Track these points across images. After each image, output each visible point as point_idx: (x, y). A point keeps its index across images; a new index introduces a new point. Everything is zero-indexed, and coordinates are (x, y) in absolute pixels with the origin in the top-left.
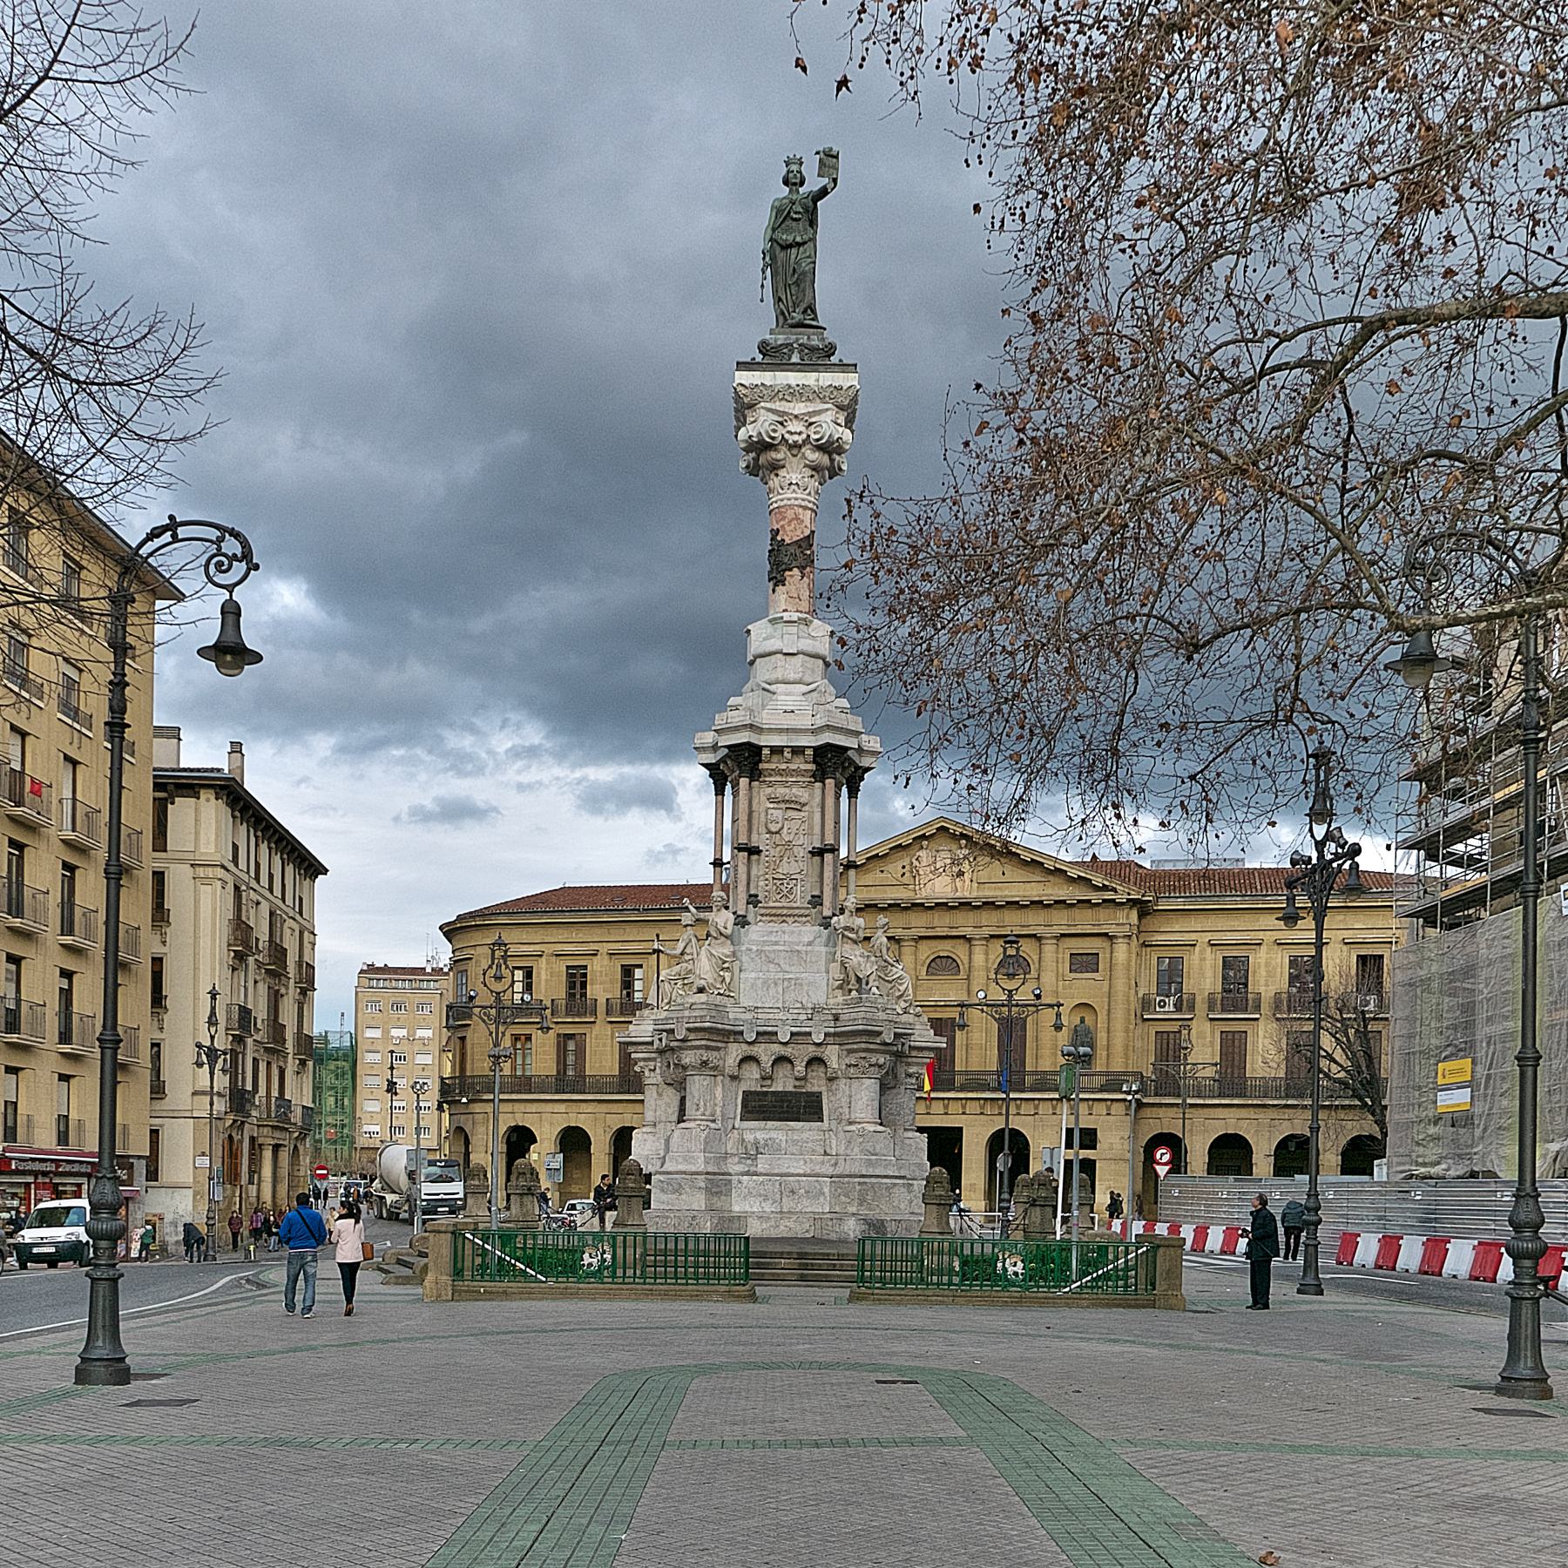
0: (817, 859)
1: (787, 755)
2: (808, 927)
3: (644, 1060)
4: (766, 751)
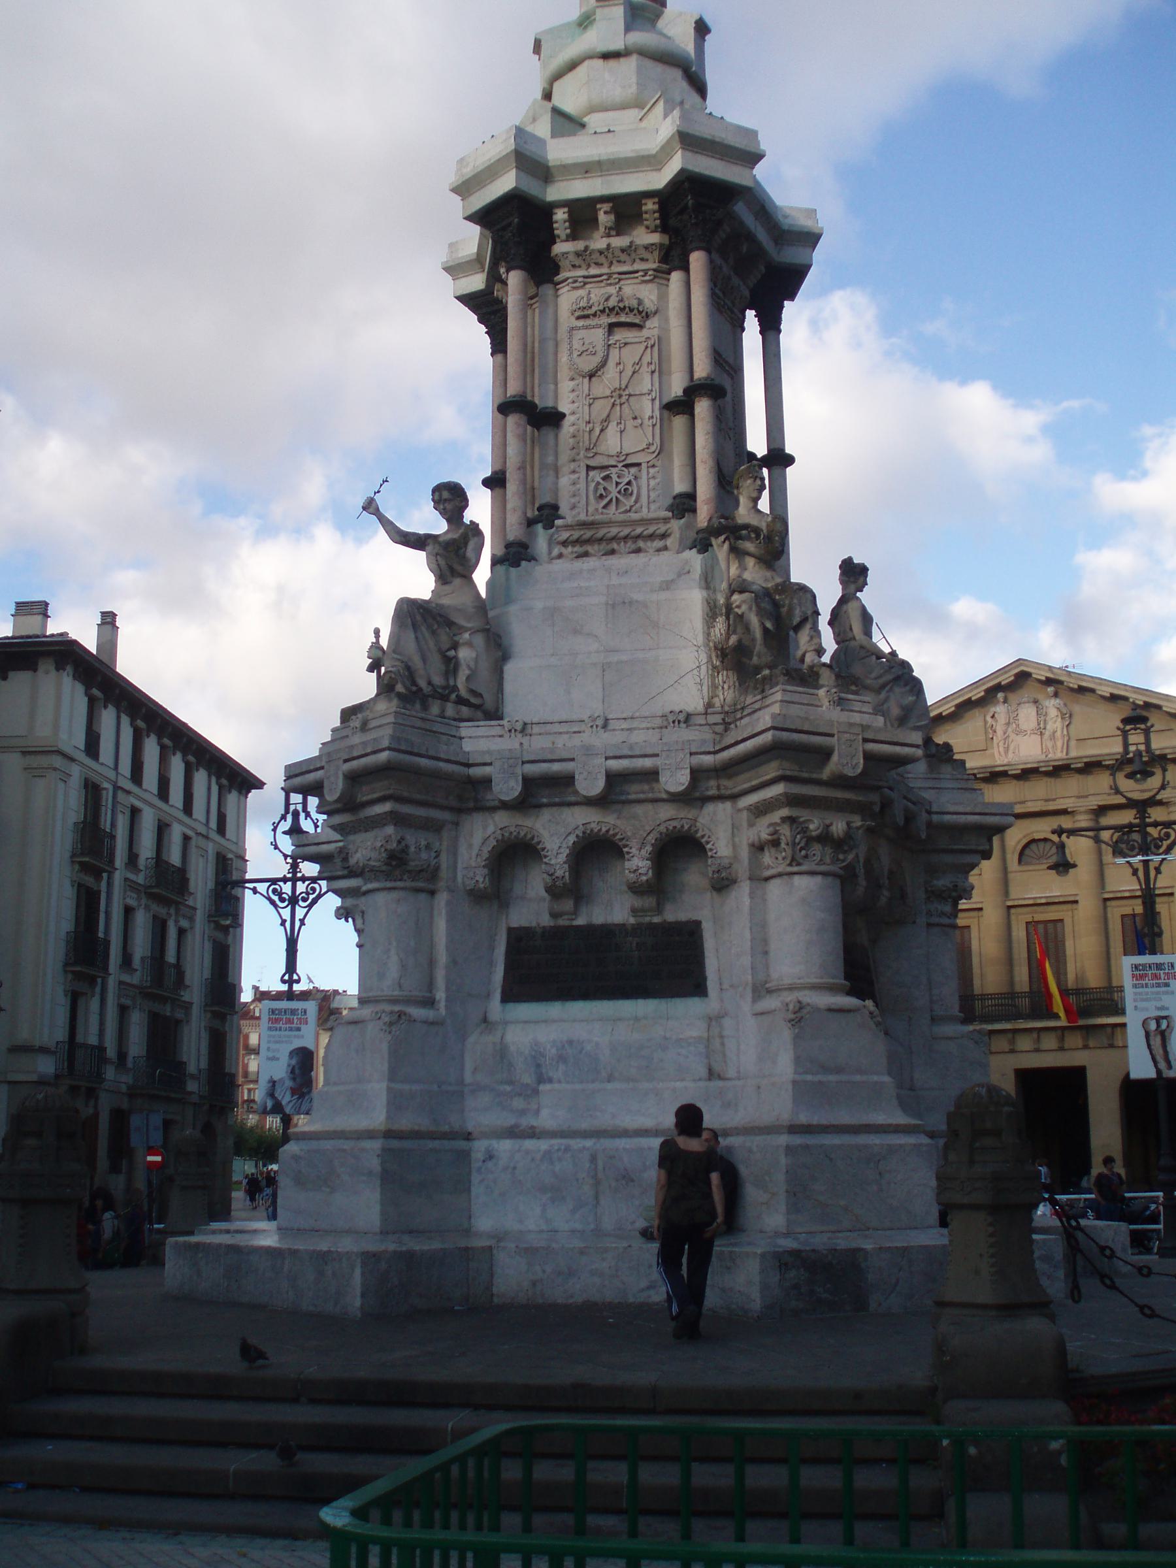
0: (679, 422)
1: (604, 218)
4: (560, 215)
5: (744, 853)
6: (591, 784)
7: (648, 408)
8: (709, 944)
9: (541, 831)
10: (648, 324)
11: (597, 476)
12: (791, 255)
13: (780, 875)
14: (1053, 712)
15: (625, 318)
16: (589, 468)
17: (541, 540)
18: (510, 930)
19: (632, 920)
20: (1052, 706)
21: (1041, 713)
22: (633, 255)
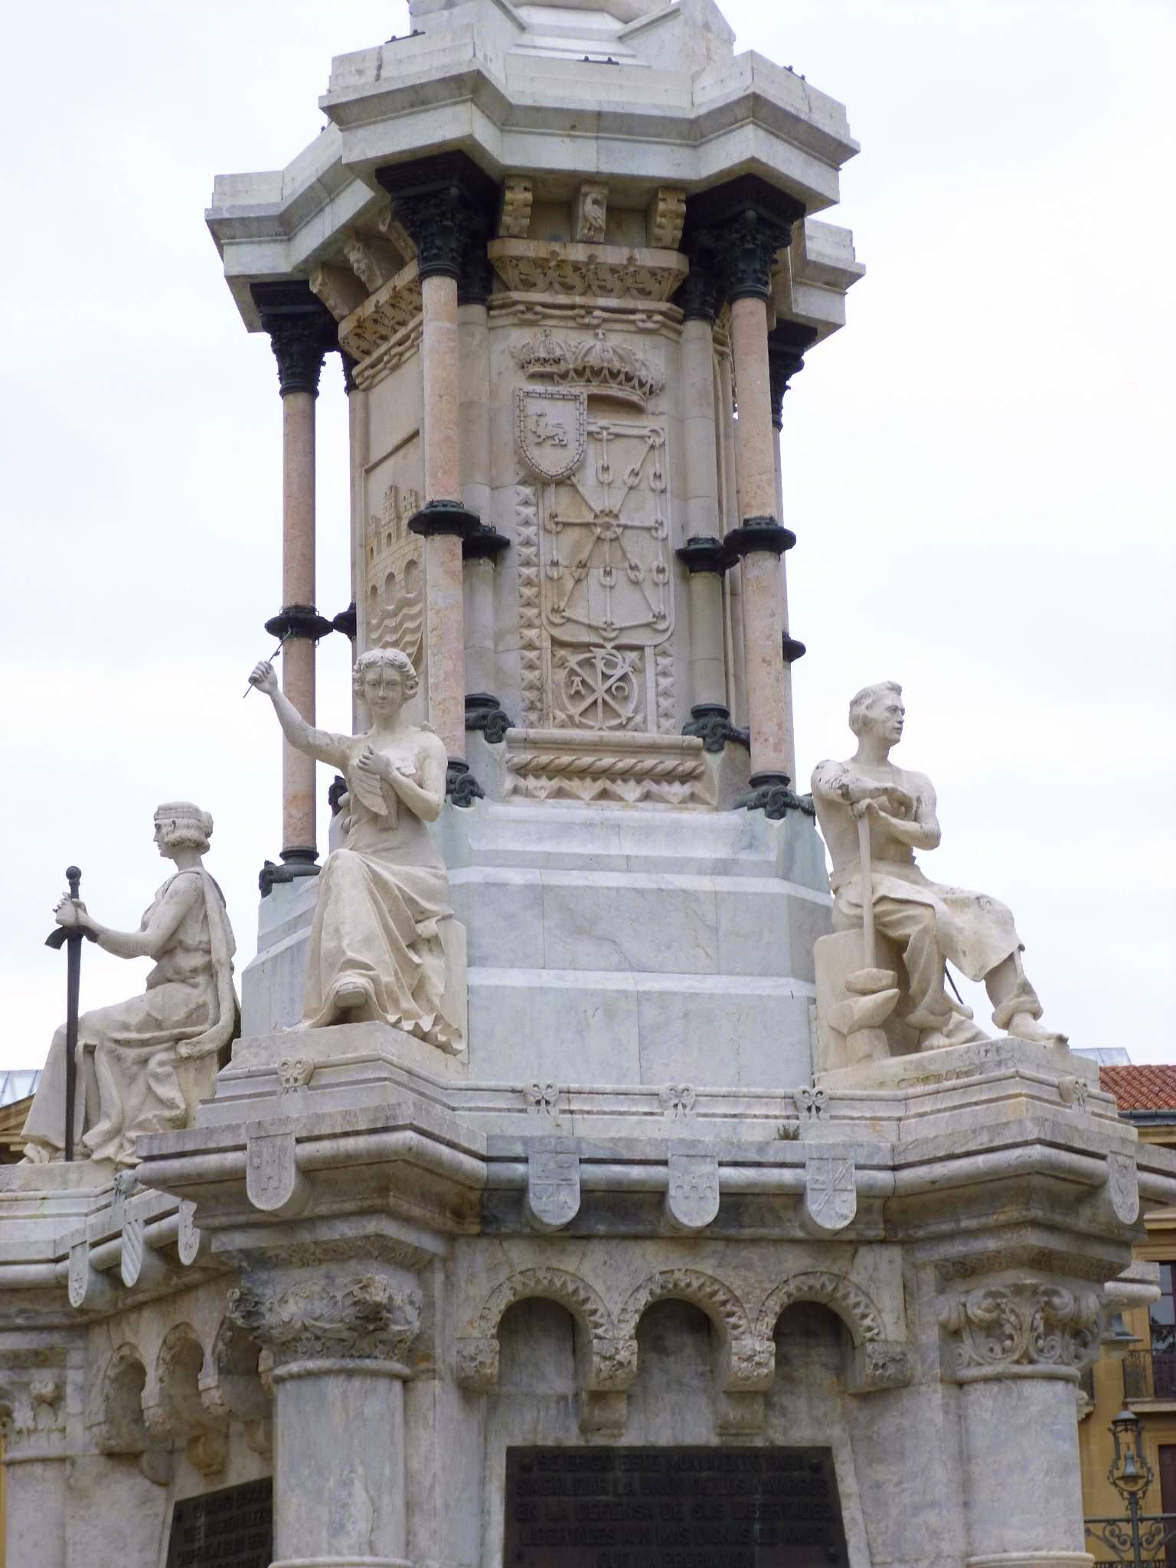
1: (592, 210)
2: (697, 816)
4: (517, 197)
5: (931, 1336)
6: (694, 1206)
7: (654, 556)
8: (848, 1483)
9: (591, 1280)
10: (650, 406)
11: (574, 659)
12: (807, 304)
13: (998, 1379)
15: (613, 393)
16: (556, 643)
17: (490, 761)
18: (511, 1452)
19: (714, 1441)
22: (629, 281)
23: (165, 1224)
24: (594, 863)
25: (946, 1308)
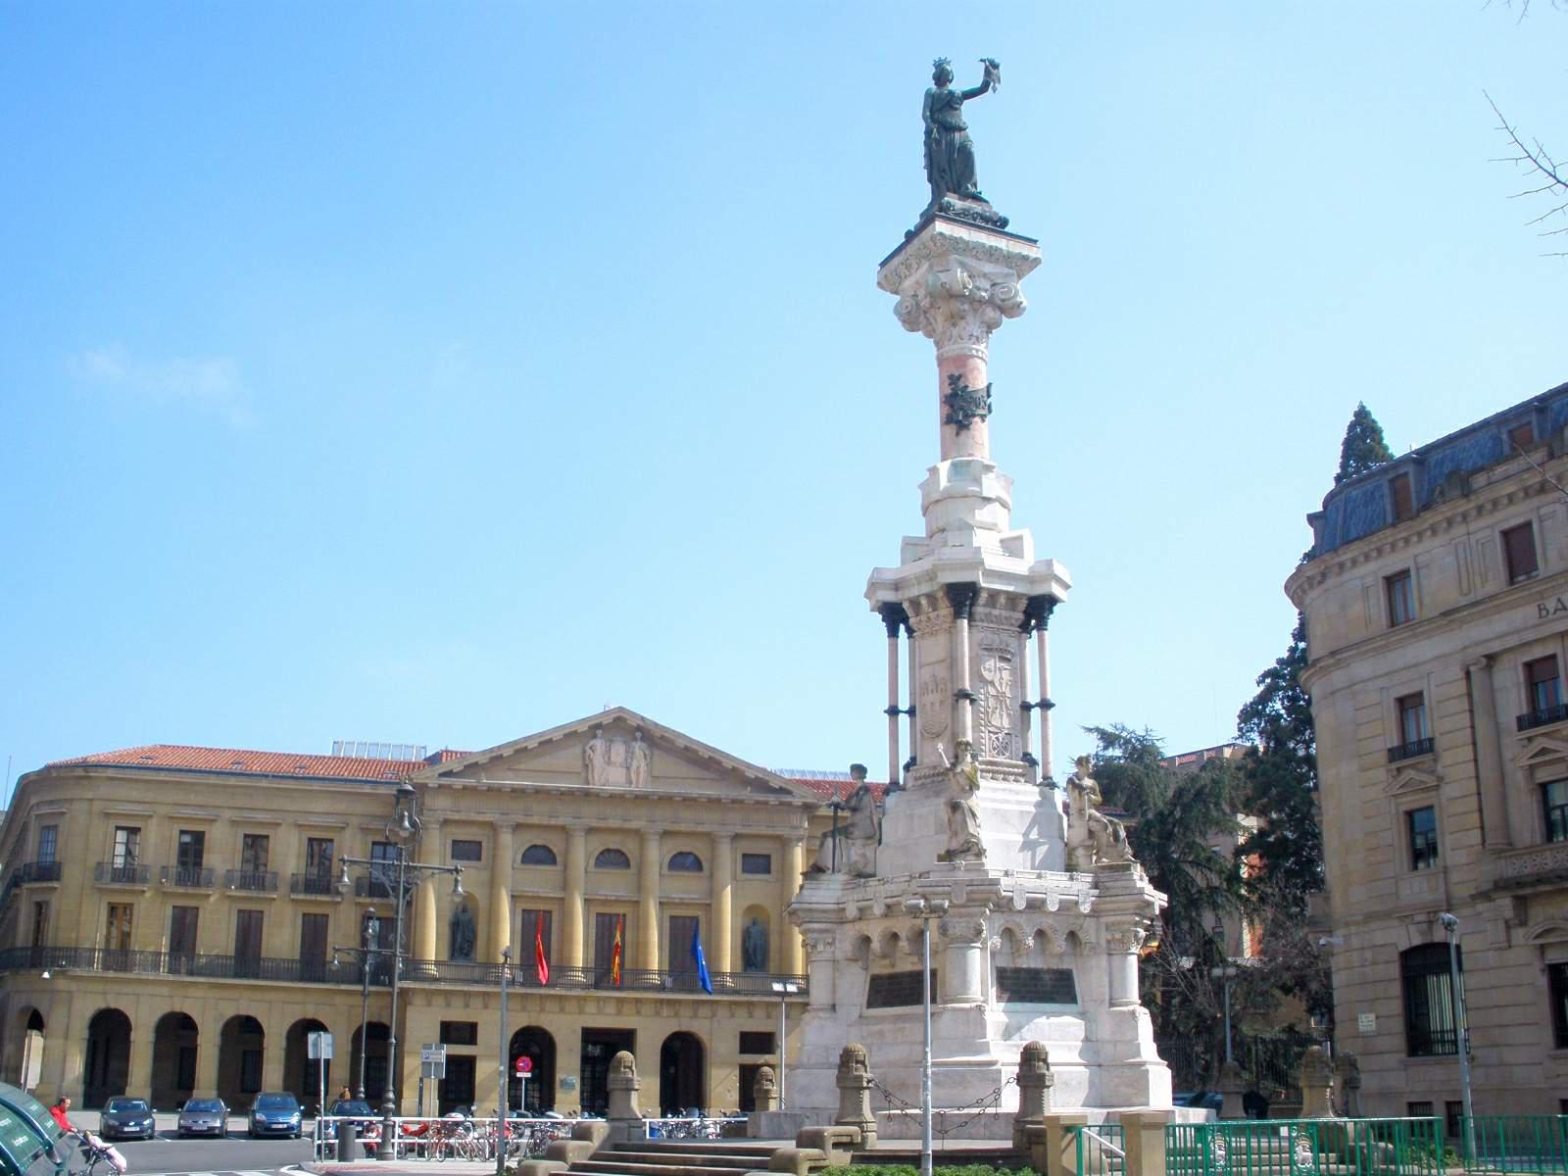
1: (1002, 600)
3: (821, 931)
4: (984, 595)
5: (1103, 943)
6: (1053, 907)
11: (994, 737)
14: (638, 753)
20: (639, 748)
21: (630, 753)
23: (894, 899)
24: (1007, 802)
25: (1110, 937)
